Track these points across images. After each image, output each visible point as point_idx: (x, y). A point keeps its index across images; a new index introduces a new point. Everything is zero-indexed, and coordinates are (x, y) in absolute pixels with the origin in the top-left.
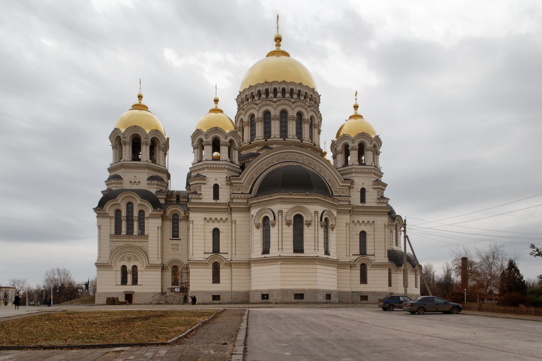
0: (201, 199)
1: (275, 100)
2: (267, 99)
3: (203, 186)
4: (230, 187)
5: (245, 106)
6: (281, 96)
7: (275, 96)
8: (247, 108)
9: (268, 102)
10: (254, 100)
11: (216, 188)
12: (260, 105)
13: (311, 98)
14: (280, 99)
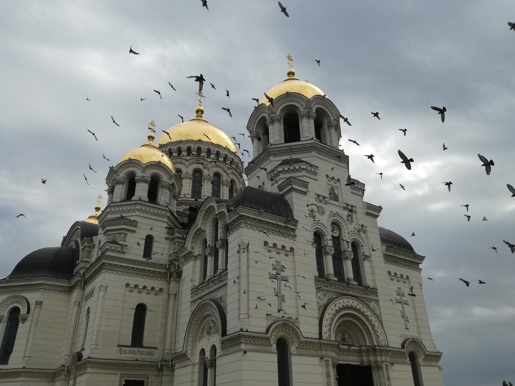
0: (124, 253)
3: (129, 234)
4: (170, 243)
11: (149, 240)
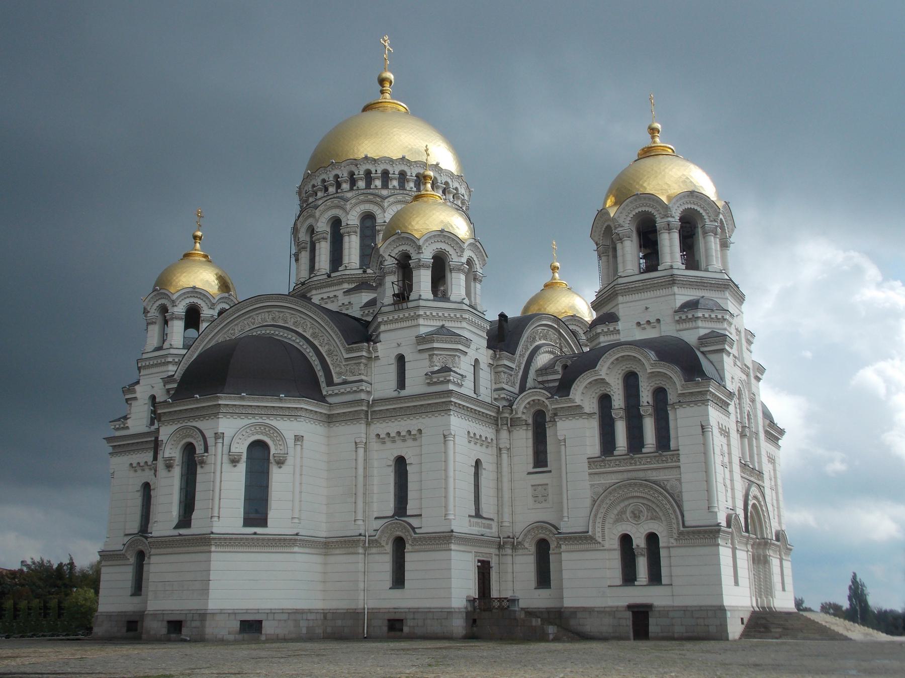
1: (385, 192)
2: (369, 191)
5: (320, 202)
6: (398, 188)
7: (385, 186)
8: (326, 205)
9: (370, 197)
10: (339, 191)
12: (353, 201)
13: (456, 194)
14: (396, 192)
